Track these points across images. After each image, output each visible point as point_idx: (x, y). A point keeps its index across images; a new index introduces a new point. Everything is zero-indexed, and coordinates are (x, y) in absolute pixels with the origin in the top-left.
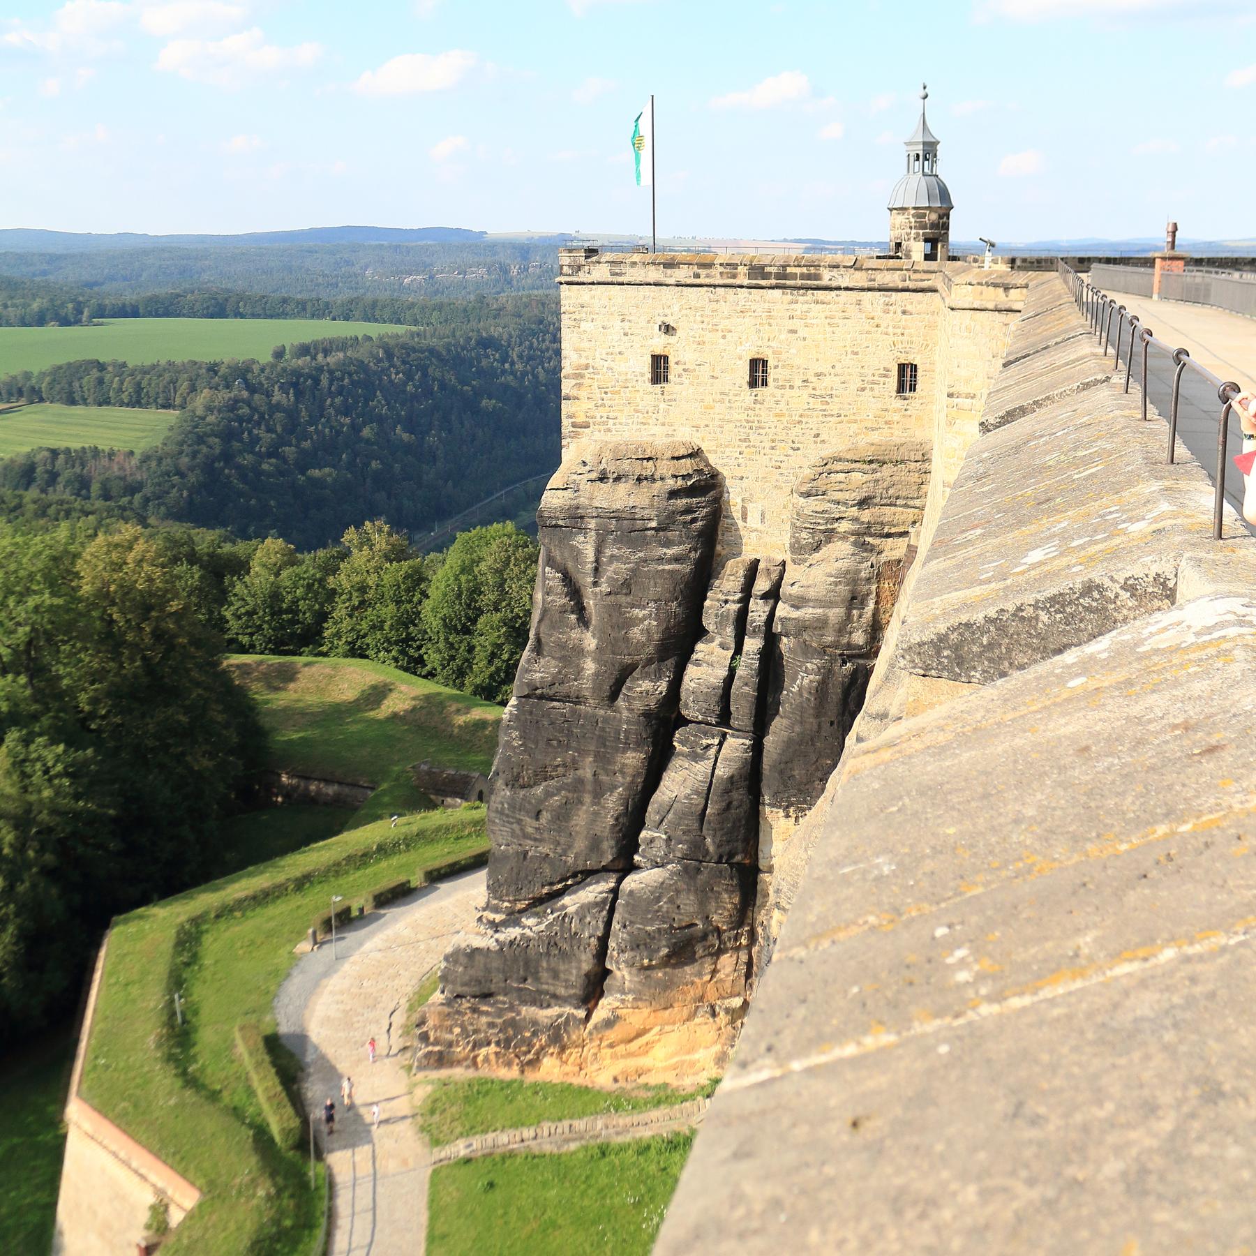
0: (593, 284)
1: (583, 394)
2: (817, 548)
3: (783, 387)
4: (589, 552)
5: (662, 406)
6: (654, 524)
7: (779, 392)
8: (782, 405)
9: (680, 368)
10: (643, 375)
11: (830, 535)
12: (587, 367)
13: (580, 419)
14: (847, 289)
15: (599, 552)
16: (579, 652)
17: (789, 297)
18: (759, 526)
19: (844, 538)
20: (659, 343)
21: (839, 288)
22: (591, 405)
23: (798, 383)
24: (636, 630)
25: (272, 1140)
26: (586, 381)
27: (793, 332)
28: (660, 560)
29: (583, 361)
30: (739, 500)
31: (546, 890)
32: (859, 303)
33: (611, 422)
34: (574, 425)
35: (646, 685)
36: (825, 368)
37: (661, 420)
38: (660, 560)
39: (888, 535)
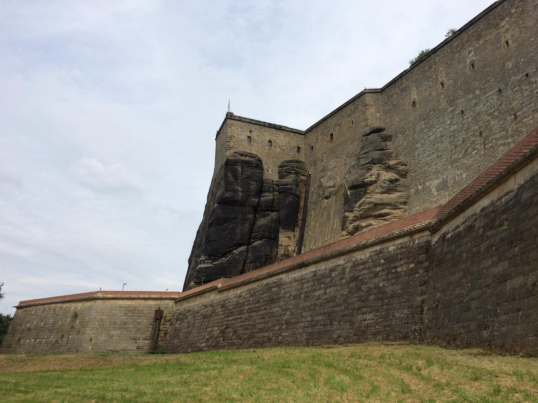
0: (235, 120)
1: (232, 141)
2: (287, 176)
3: (275, 147)
4: (240, 169)
5: (249, 147)
6: (255, 165)
7: (274, 148)
8: (275, 150)
9: (254, 140)
10: (245, 140)
11: (290, 173)
12: (233, 136)
13: (231, 146)
14: (287, 131)
15: (242, 169)
16: (237, 191)
17: (276, 131)
18: (271, 173)
19: (293, 173)
20: (249, 134)
21: (286, 130)
22: (233, 144)
23: (278, 146)
24: (252, 186)
25: (232, 252)
26: (232, 139)
27: (277, 137)
28: (257, 172)
29: (232, 135)
30: (267, 167)
31: (227, 250)
32: (289, 134)
33: (238, 148)
34: (229, 147)
35: (254, 199)
36: (283, 145)
37: (249, 149)
38: (257, 172)
39: (301, 175)
